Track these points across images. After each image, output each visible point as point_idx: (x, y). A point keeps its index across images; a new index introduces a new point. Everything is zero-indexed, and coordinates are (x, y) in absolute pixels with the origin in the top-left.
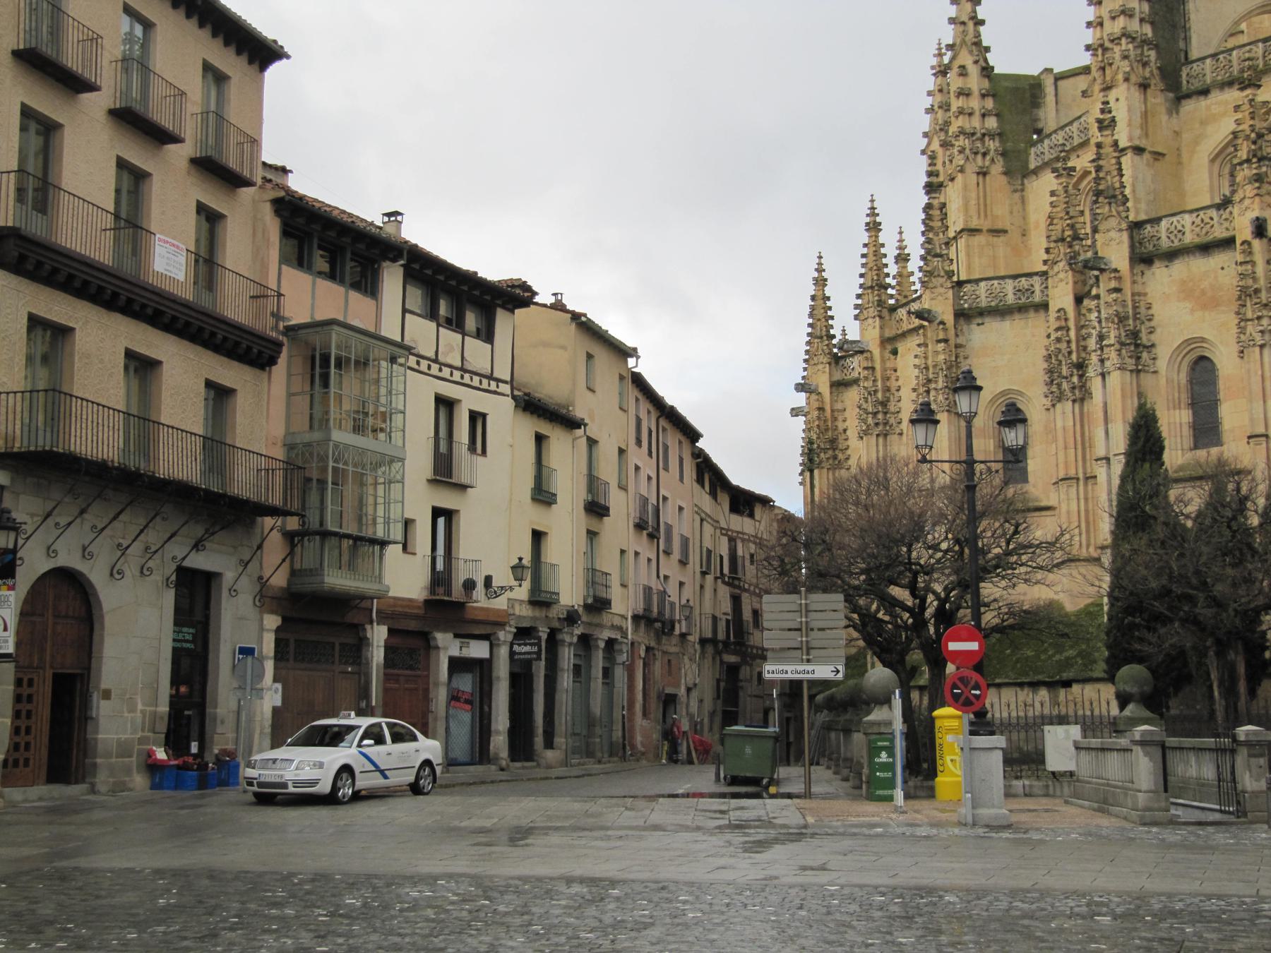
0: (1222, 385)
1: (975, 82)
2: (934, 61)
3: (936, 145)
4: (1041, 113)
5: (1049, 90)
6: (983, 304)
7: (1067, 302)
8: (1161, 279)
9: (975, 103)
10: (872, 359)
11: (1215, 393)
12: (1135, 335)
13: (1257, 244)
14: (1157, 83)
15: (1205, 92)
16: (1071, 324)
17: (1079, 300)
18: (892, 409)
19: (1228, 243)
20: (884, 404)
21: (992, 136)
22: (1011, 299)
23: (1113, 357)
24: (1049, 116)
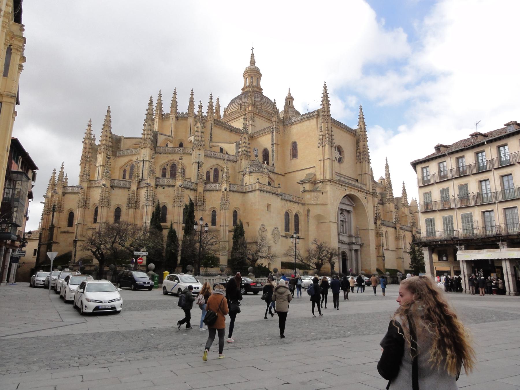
0: (168, 211)
1: (109, 135)
2: (89, 123)
3: (87, 141)
4: (120, 144)
5: (122, 140)
6: (116, 185)
7: (135, 189)
8: (160, 189)
9: (108, 139)
10: (84, 191)
11: (166, 212)
12: (154, 199)
13: (180, 188)
14: (153, 149)
15: (160, 153)
16: (135, 193)
17: (137, 189)
18: (88, 202)
19: (173, 186)
20: (86, 201)
21: (110, 146)
22: (122, 185)
23: (150, 203)
24: (122, 146)
